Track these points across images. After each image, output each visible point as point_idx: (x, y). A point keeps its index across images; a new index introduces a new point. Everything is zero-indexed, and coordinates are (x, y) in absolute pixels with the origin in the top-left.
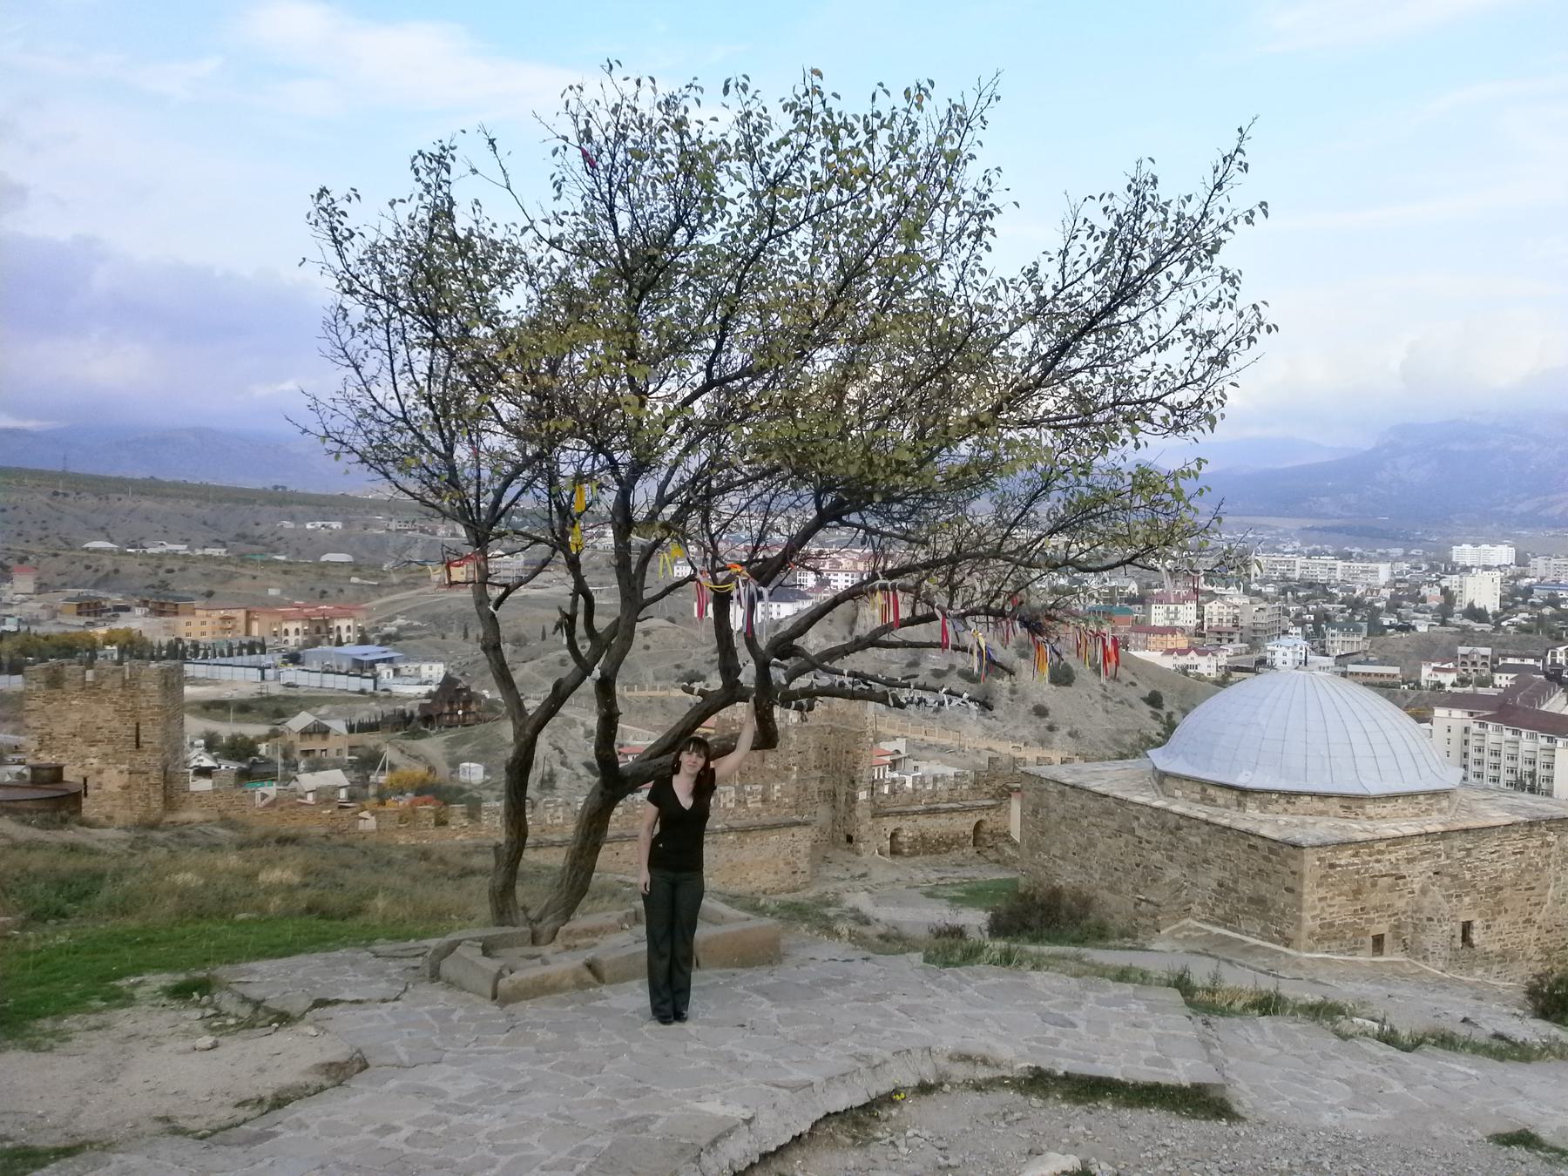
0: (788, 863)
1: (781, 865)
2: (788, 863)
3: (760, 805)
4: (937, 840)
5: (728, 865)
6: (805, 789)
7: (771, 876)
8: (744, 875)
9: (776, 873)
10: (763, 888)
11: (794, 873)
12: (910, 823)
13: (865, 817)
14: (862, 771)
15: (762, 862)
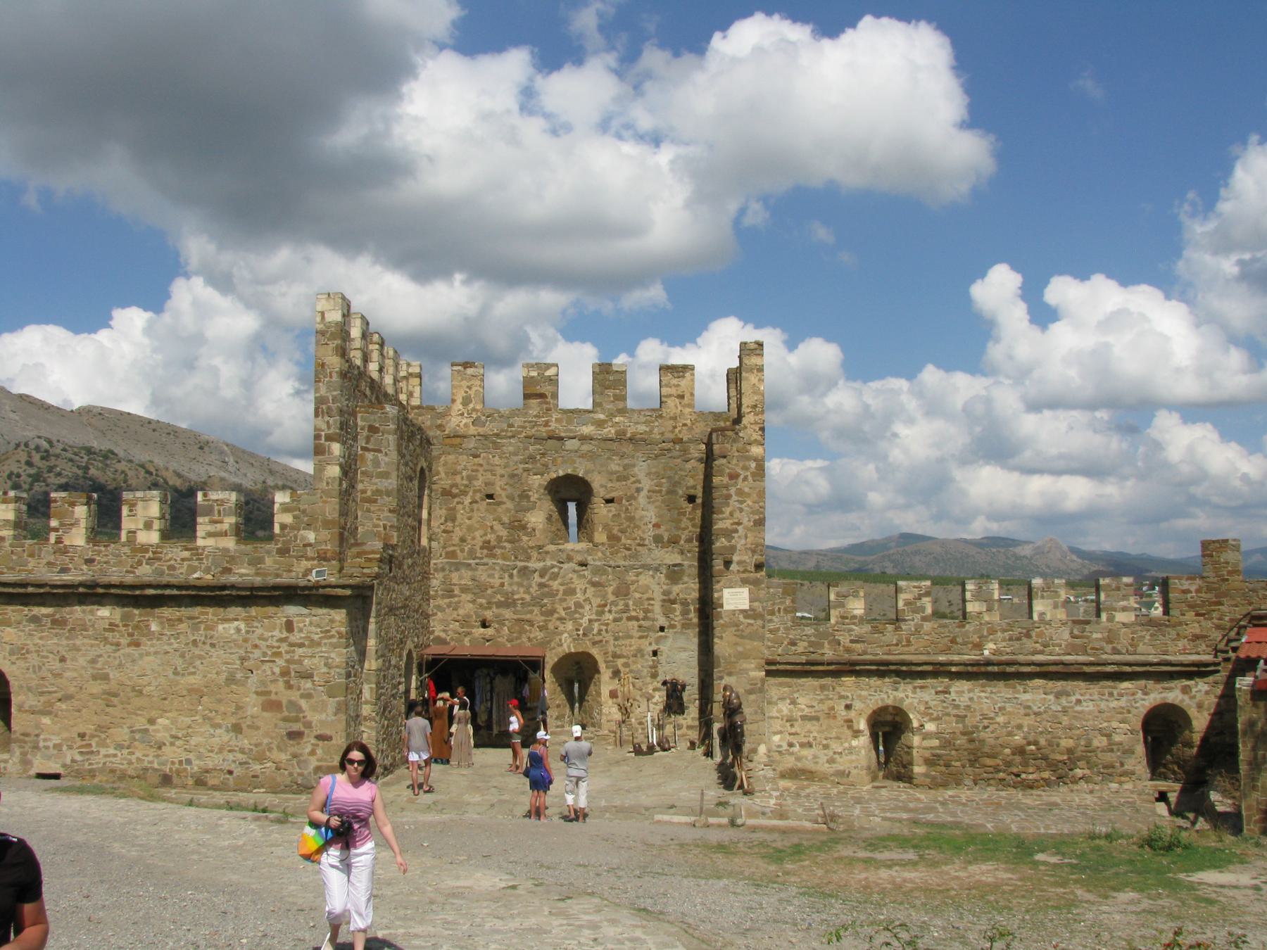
0: (272, 705)
1: (253, 706)
2: (272, 705)
3: (230, 543)
4: (1020, 751)
5: (97, 688)
6: (623, 591)
7: (222, 736)
8: (141, 723)
9: (237, 729)
10: (196, 766)
11: (295, 736)
12: (928, 696)
13: (745, 656)
14: (729, 534)
15: (197, 693)
